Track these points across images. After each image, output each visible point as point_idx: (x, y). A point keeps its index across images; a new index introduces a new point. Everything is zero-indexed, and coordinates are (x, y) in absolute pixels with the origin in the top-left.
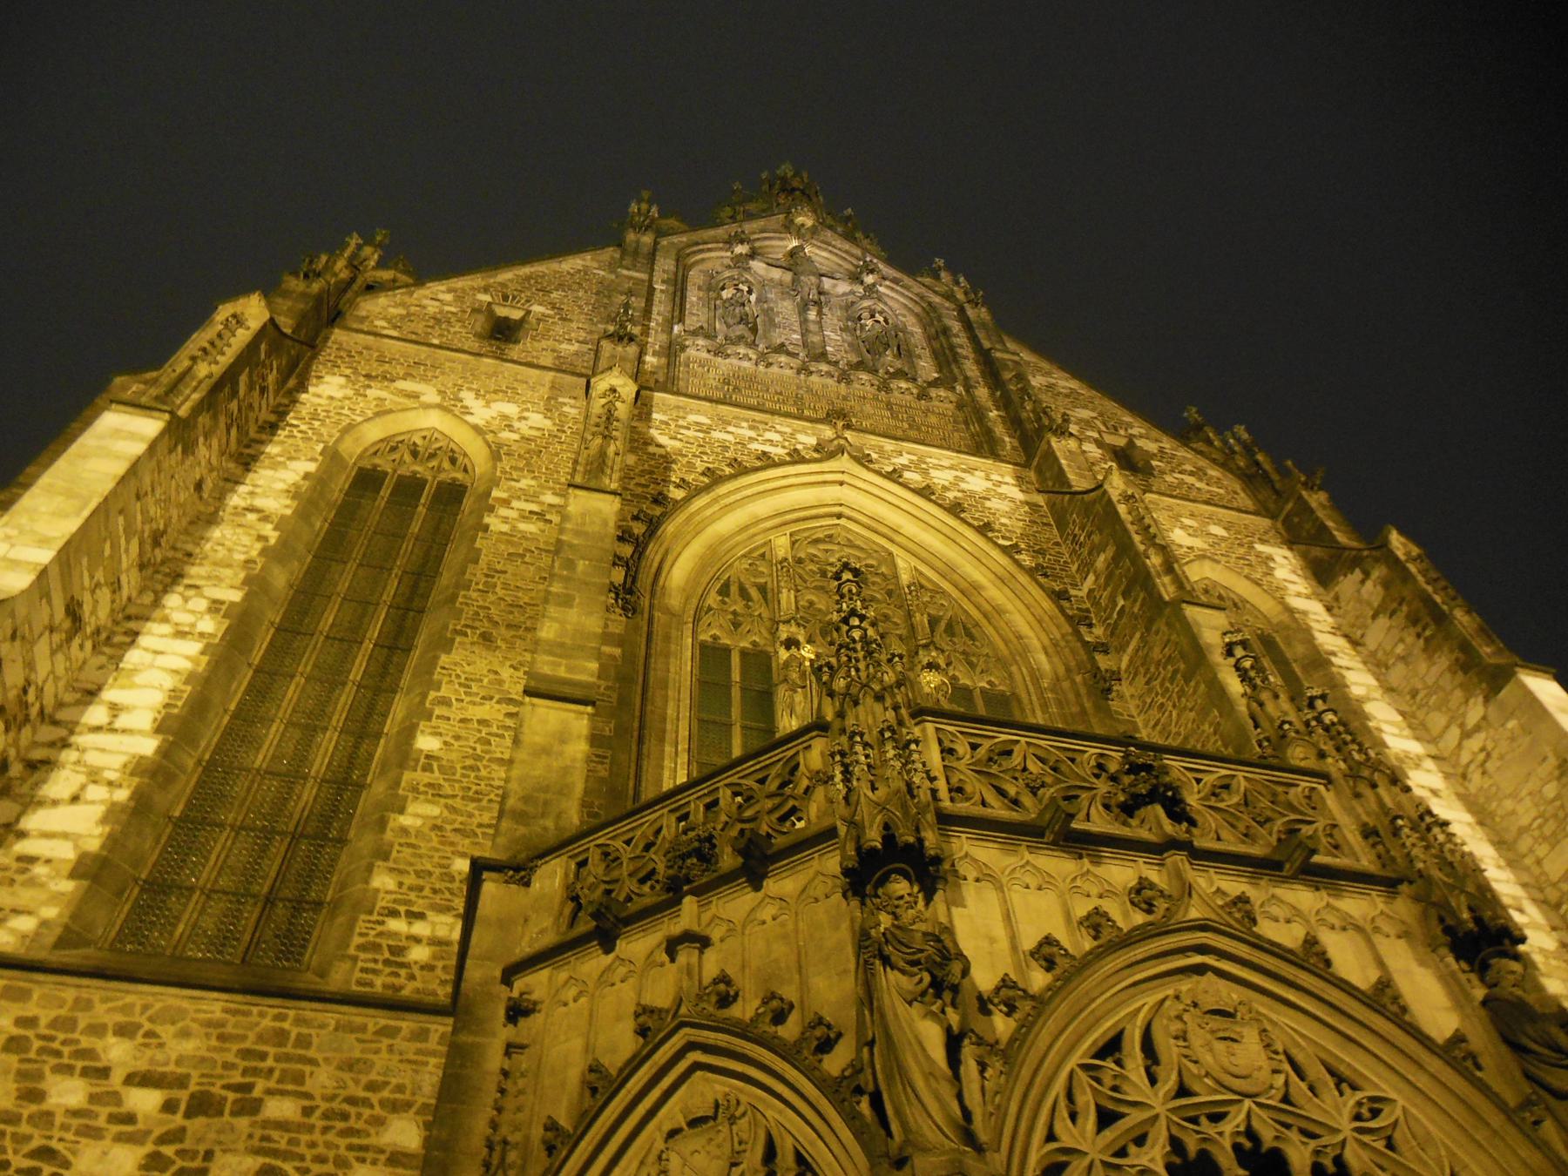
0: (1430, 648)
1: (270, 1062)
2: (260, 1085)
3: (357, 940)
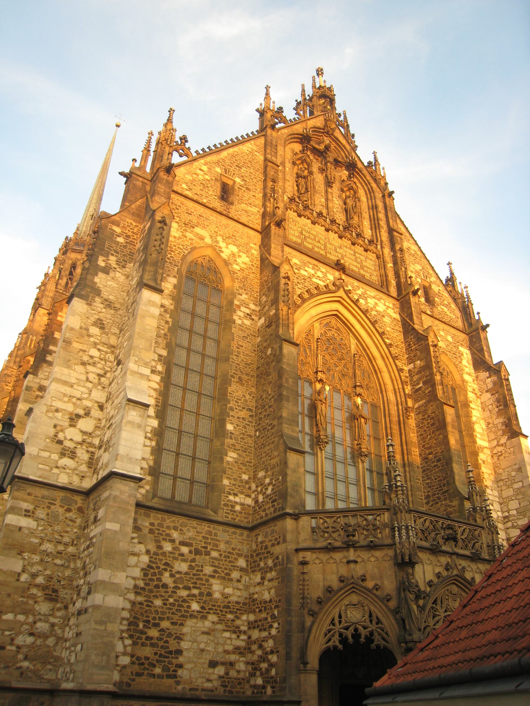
0: (499, 414)
1: (209, 541)
2: (209, 547)
3: (223, 503)
